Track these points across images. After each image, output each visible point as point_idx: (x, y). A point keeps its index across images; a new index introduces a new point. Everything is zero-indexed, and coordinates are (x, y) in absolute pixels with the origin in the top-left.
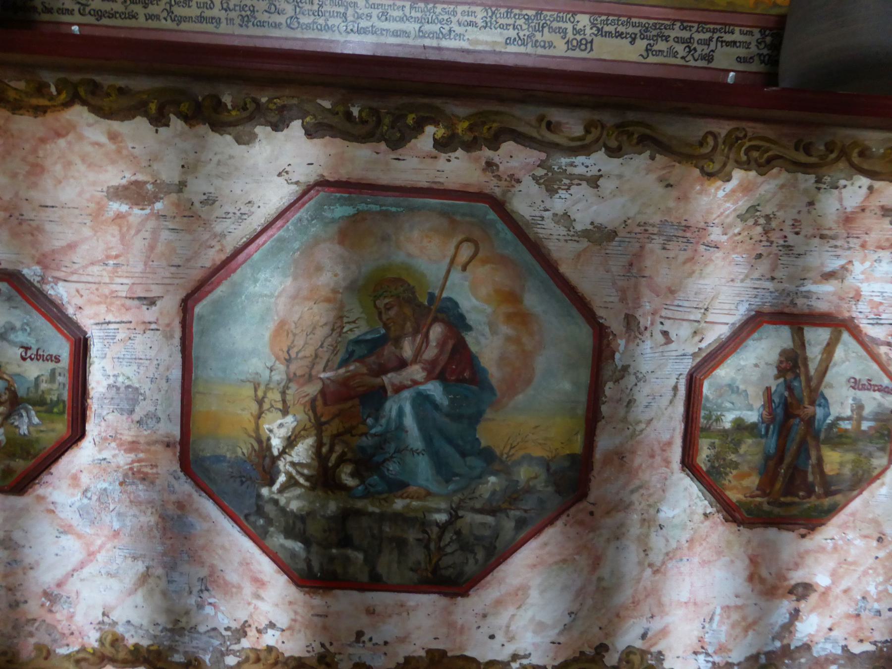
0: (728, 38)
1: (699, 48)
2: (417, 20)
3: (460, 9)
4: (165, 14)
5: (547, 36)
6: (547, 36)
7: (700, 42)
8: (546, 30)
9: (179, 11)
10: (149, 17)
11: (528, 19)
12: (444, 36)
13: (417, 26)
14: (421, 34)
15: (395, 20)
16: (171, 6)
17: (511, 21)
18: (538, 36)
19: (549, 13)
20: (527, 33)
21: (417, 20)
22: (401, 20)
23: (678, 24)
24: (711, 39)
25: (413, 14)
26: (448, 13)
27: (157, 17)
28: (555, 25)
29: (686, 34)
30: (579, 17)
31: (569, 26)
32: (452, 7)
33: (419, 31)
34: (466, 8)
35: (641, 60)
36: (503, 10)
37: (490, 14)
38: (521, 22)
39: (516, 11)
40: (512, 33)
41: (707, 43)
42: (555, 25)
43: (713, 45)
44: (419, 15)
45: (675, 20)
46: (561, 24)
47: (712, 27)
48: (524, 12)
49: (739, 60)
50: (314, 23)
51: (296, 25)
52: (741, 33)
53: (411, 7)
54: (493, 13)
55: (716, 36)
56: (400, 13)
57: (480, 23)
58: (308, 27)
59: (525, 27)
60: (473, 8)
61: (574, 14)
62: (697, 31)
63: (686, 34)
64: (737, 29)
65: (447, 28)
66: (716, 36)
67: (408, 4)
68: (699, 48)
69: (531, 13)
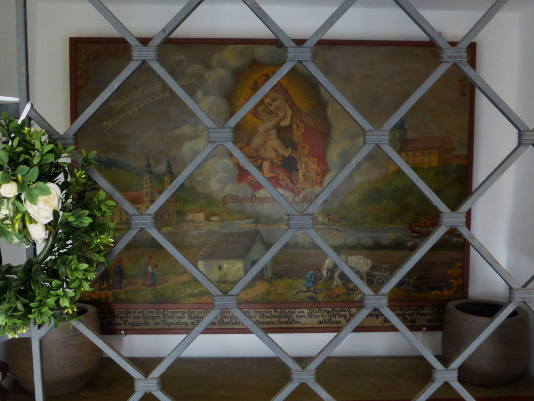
0: (422, 312)
1: (409, 318)
2: (277, 317)
3: (297, 310)
4: (163, 322)
5: (337, 319)
6: (337, 319)
7: (409, 315)
8: (337, 316)
9: (168, 320)
10: (156, 324)
11: (328, 312)
12: (290, 323)
13: (277, 319)
14: (280, 323)
15: (267, 317)
16: (165, 319)
17: (321, 314)
18: (333, 319)
19: (338, 309)
20: (328, 318)
21: (277, 317)
22: (270, 317)
23: (398, 308)
24: (414, 313)
25: (276, 314)
26: (291, 313)
27: (159, 324)
28: (341, 313)
29: (402, 312)
30: (351, 309)
31: (347, 313)
32: (293, 310)
33: (279, 321)
34: (299, 310)
35: (382, 325)
36: (316, 309)
37: (311, 311)
38: (325, 313)
39: (323, 309)
40: (321, 319)
41: (412, 315)
42: (341, 313)
43: (415, 316)
44: (278, 314)
45: (396, 306)
46: (344, 313)
47: (414, 308)
48: (327, 309)
49: (428, 321)
50: (230, 321)
51: (222, 323)
52: (428, 309)
53: (275, 311)
54: (312, 311)
55: (416, 312)
56: (269, 314)
57: (306, 316)
58: (228, 323)
59: (327, 315)
60: (303, 310)
61: (350, 308)
62: (408, 310)
63: (402, 312)
64: (426, 308)
65: (291, 319)
66: (416, 312)
67: (273, 310)
68: (409, 318)
69: (330, 309)
